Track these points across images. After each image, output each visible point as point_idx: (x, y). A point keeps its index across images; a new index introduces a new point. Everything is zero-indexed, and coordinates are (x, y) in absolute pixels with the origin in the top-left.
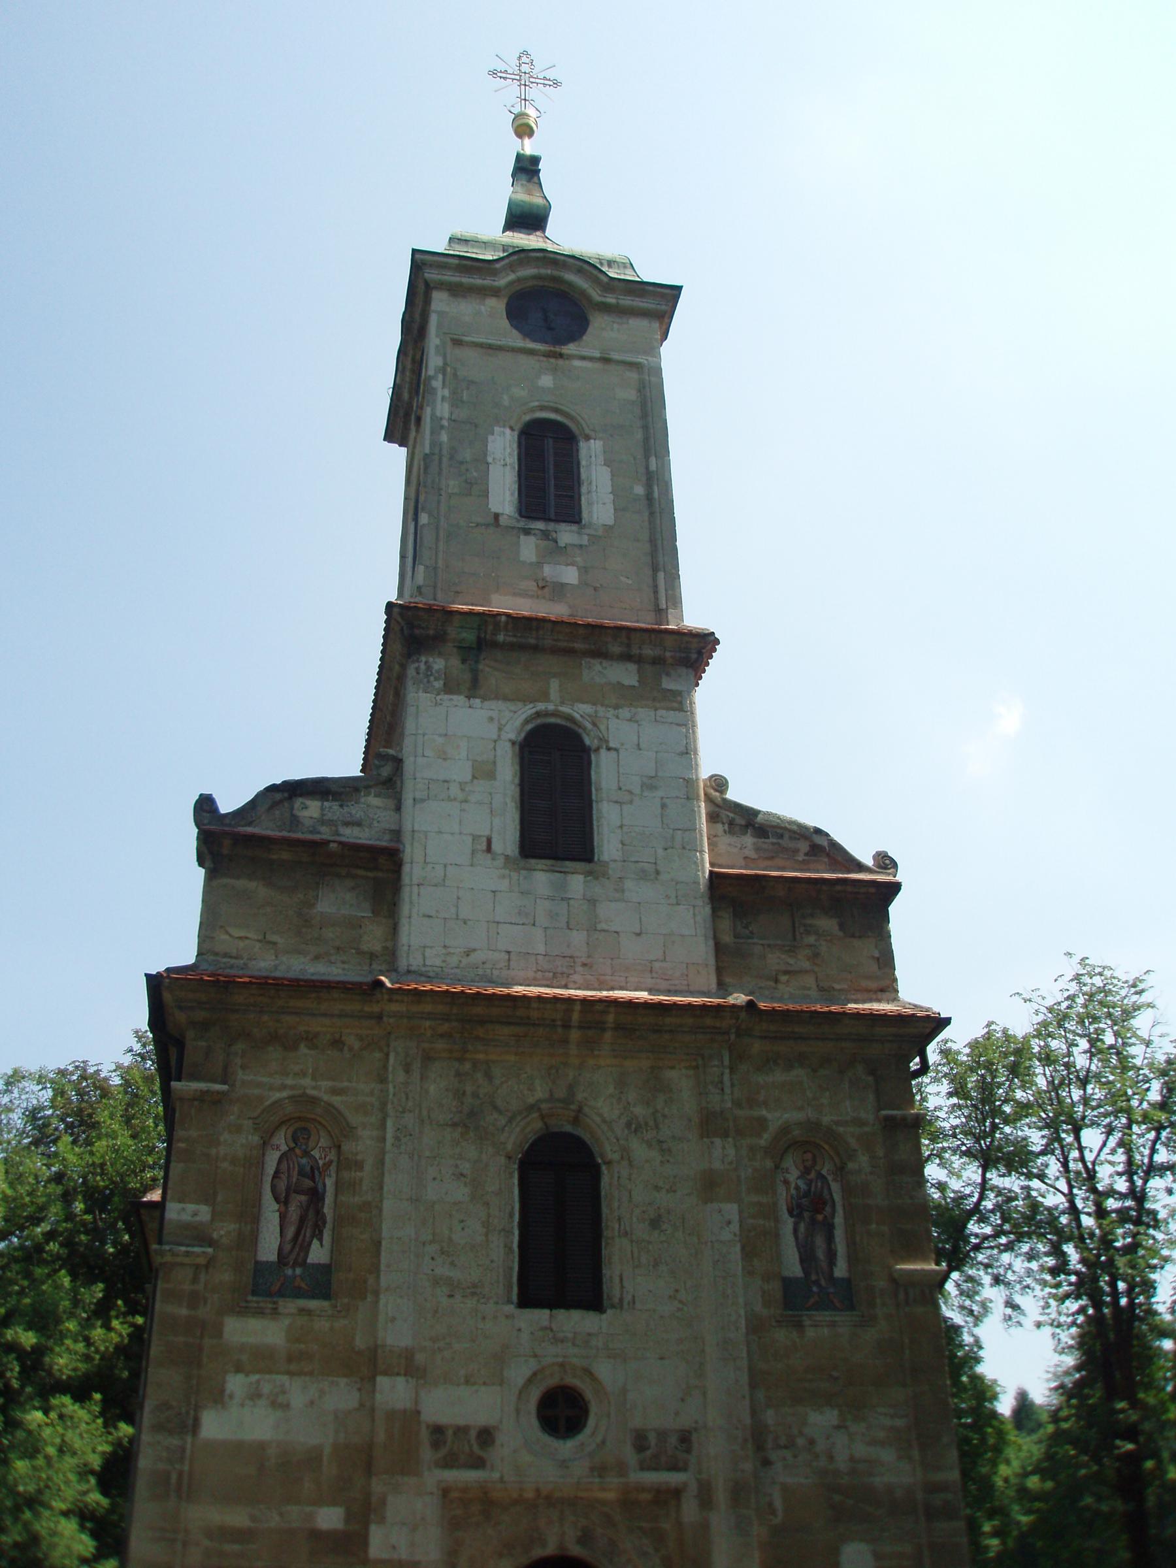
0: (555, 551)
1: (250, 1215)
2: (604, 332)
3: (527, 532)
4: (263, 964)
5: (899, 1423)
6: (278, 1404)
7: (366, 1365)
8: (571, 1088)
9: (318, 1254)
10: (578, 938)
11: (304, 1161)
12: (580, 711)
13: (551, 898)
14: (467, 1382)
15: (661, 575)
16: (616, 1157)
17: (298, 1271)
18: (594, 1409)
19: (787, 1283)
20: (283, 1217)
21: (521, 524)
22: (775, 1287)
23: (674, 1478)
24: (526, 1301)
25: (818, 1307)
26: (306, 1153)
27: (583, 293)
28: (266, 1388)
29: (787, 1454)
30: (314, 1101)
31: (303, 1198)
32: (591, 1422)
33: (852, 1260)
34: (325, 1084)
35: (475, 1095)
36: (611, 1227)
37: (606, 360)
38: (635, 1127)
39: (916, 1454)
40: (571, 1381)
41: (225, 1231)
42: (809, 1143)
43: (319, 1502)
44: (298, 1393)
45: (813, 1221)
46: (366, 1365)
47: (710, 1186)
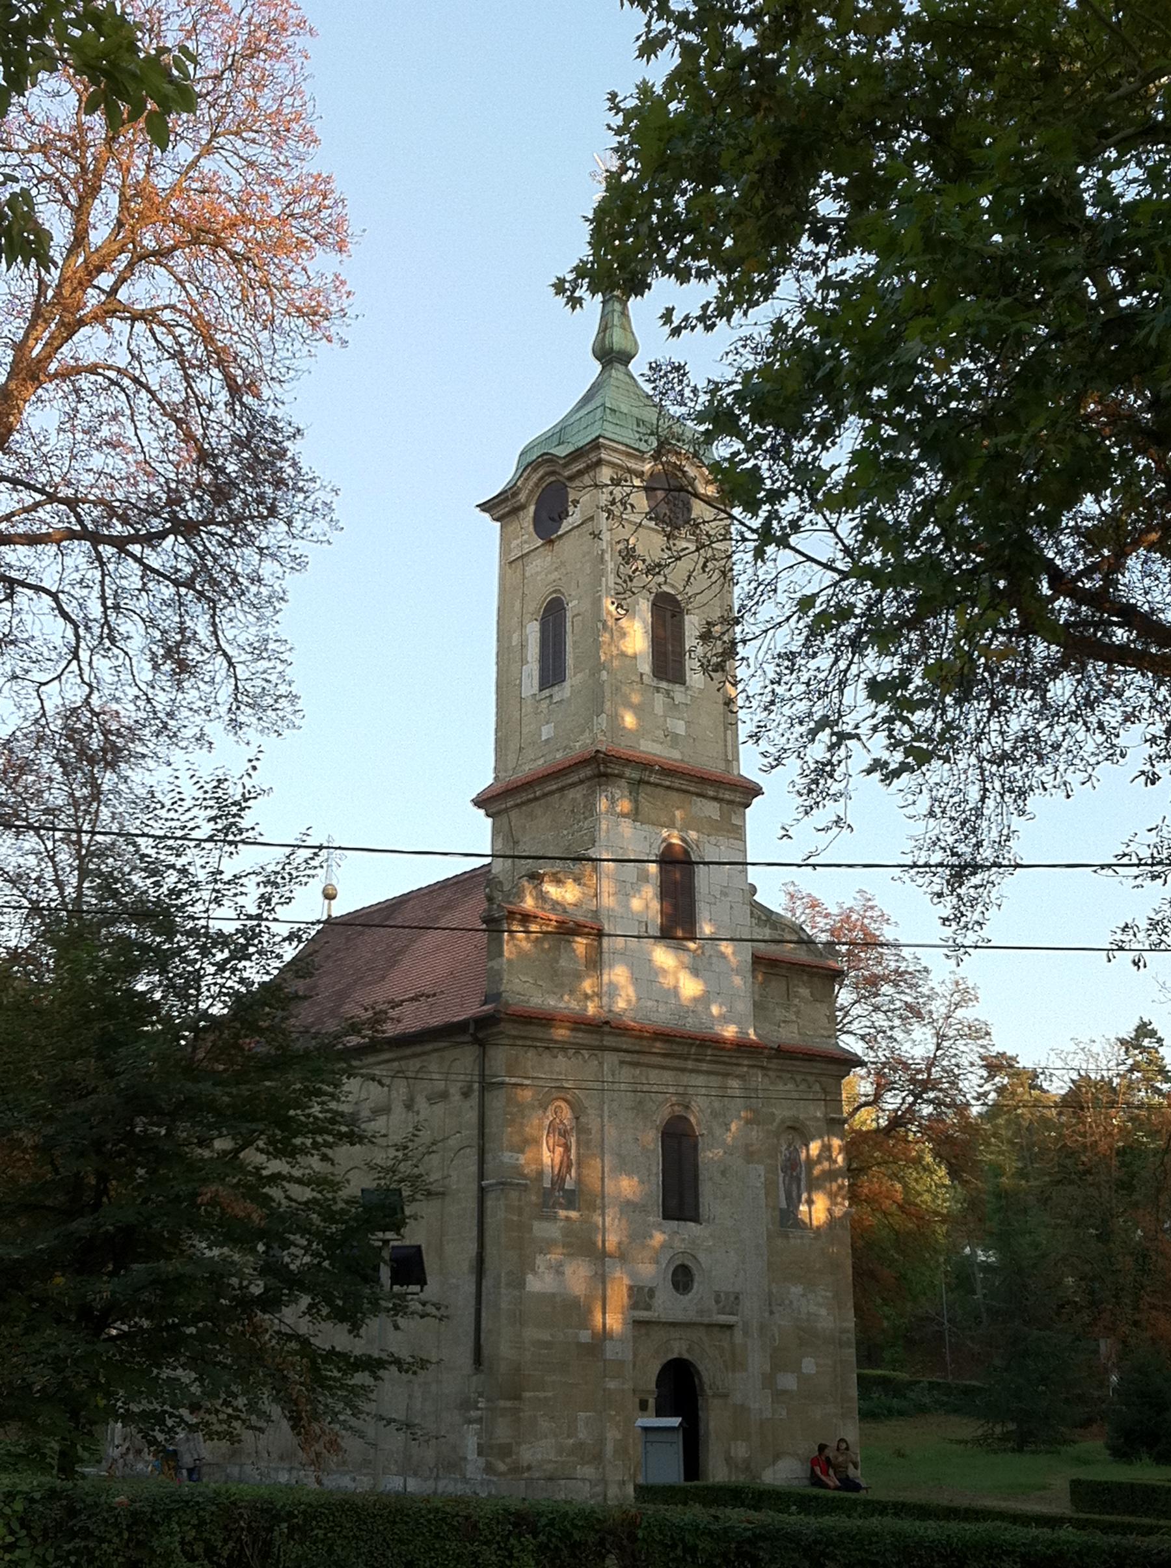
0: (673, 707)
3: (658, 690)
18: (697, 1278)
22: (777, 1213)
23: (732, 1319)
24: (666, 1217)
32: (695, 1285)
36: (704, 1175)
40: (687, 1263)
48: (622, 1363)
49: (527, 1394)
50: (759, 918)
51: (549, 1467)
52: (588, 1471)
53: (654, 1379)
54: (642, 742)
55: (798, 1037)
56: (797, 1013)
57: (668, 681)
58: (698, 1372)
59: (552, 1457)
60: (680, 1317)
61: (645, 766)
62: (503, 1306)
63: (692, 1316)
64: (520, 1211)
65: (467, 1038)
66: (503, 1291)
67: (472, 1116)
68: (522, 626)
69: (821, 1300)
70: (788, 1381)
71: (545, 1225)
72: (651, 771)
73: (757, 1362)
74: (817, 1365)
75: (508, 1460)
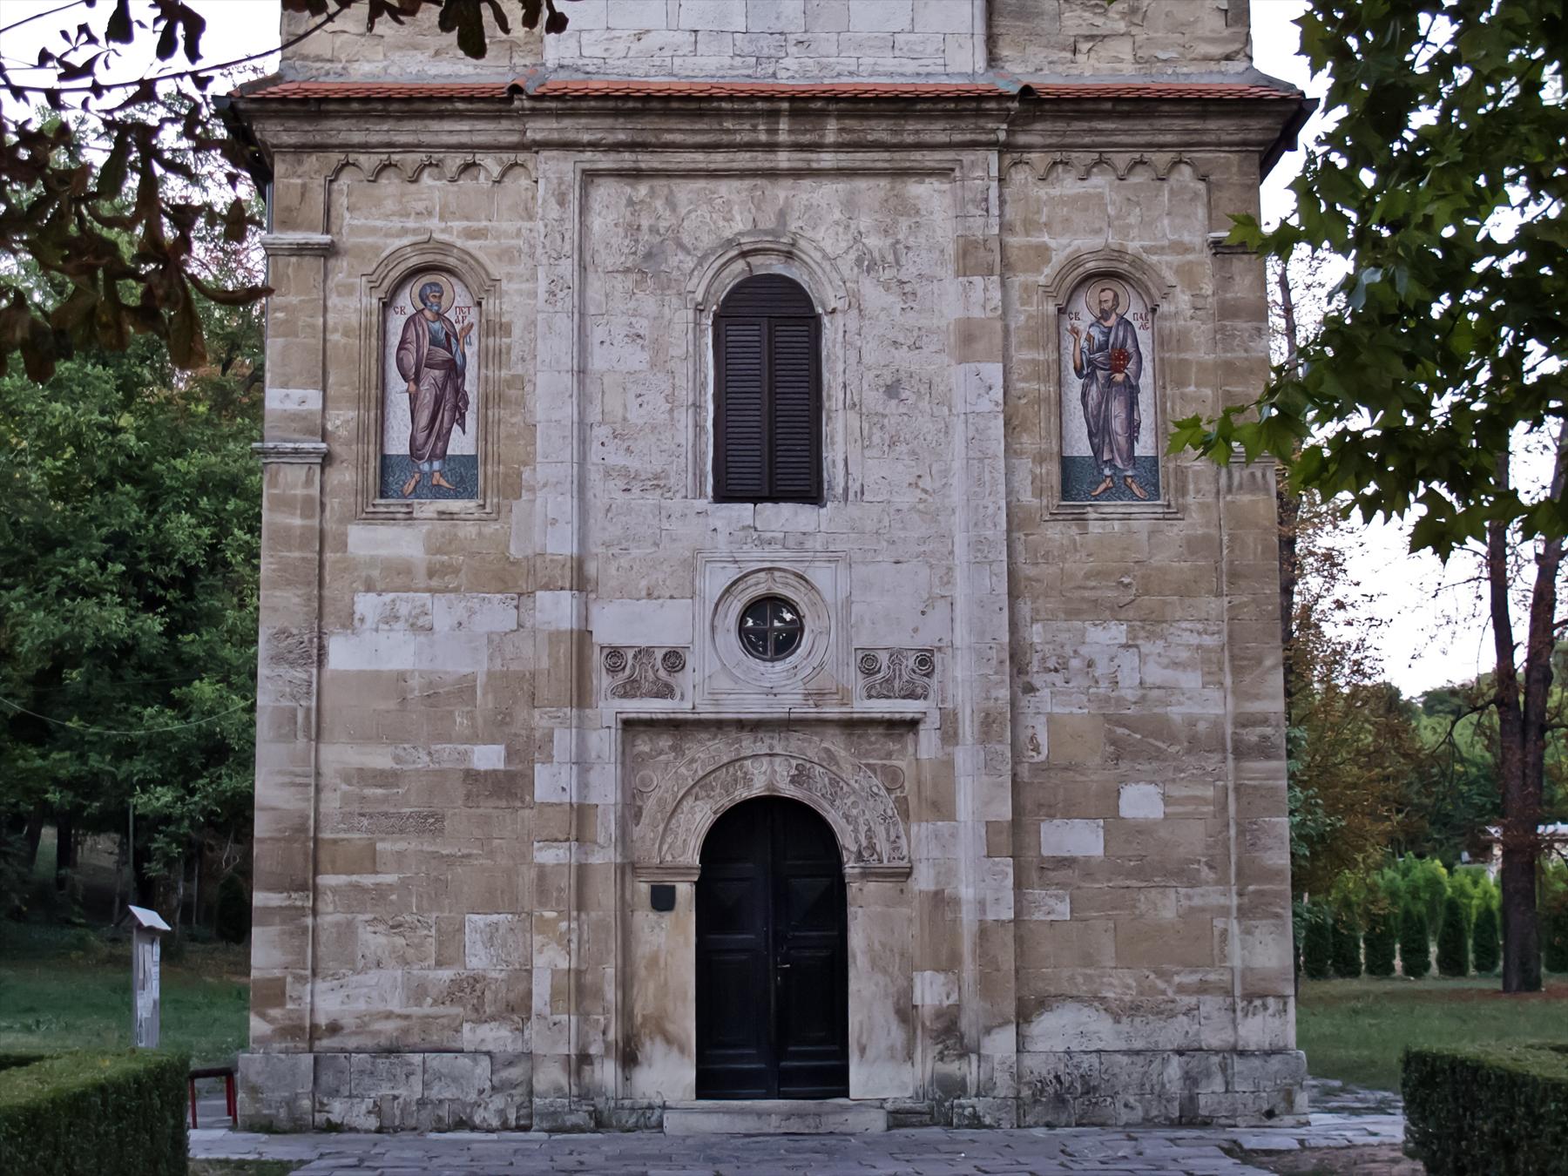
11: (437, 326)
17: (436, 465)
20: (413, 399)
29: (1058, 679)
44: (442, 612)
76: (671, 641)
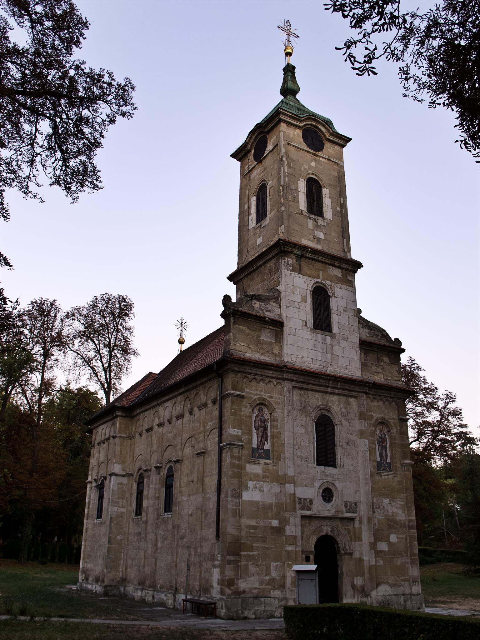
0: (317, 226)
1: (250, 434)
2: (329, 149)
4: (248, 355)
5: (402, 503)
6: (261, 491)
7: (282, 480)
8: (327, 402)
9: (267, 446)
10: (329, 356)
12: (327, 283)
13: (322, 343)
14: (306, 486)
15: (345, 240)
16: (338, 423)
19: (378, 462)
20: (257, 435)
21: (308, 215)
22: (375, 464)
23: (353, 515)
24: (318, 464)
25: (383, 470)
26: (262, 415)
27: (323, 133)
28: (258, 486)
29: (378, 510)
30: (265, 399)
31: (262, 429)
32: (334, 498)
33: (392, 458)
34: (267, 395)
35: (305, 401)
36: (338, 444)
37: (329, 160)
38: (343, 415)
39: (406, 512)
41: (245, 438)
42: (383, 423)
43: (273, 518)
44: (266, 487)
45: (382, 446)
46: (282, 480)
47: (361, 434)
48: (295, 537)
49: (243, 553)
50: (362, 324)
51: (256, 591)
52: (277, 593)
53: (313, 546)
54: (302, 239)
55: (383, 380)
56: (383, 369)
57: (315, 215)
58: (337, 542)
59: (257, 586)
60: (325, 513)
61: (305, 248)
62: (229, 506)
63: (332, 513)
64: (239, 459)
65: (214, 375)
66: (229, 499)
67: (216, 413)
68: (249, 200)
69: (399, 506)
70: (383, 546)
71: (254, 466)
72: (307, 251)
73: (367, 537)
74: (398, 538)
75: (232, 588)
76: (310, 497)
